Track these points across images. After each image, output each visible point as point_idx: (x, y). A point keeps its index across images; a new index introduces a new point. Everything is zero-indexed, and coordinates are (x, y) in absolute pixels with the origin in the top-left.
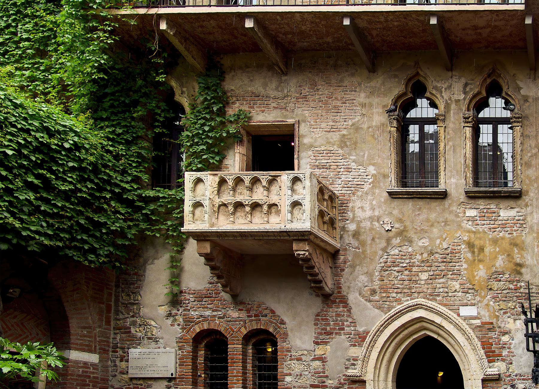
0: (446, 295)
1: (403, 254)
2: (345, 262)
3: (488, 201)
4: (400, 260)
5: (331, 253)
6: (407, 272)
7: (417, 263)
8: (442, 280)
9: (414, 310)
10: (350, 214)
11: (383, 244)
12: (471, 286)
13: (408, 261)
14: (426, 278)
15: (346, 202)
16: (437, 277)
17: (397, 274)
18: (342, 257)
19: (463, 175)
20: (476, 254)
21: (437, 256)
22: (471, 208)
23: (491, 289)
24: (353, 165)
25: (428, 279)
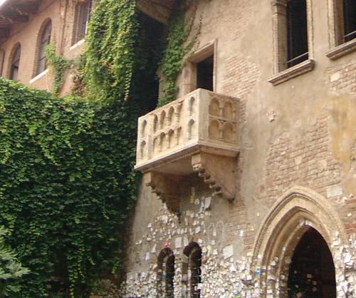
0: (315, 176)
1: (282, 141)
2: (243, 163)
3: (348, 58)
4: (280, 150)
5: (233, 158)
6: (286, 160)
7: (293, 148)
8: (313, 161)
9: (291, 199)
10: (247, 114)
11: (269, 136)
12: (336, 161)
13: (286, 148)
14: (300, 162)
15: (244, 103)
16: (309, 158)
17: (278, 164)
18: (241, 159)
19: (327, 37)
20: (340, 123)
21: (308, 135)
22: (335, 72)
23: (354, 159)
24: (249, 64)
25: (301, 164)
